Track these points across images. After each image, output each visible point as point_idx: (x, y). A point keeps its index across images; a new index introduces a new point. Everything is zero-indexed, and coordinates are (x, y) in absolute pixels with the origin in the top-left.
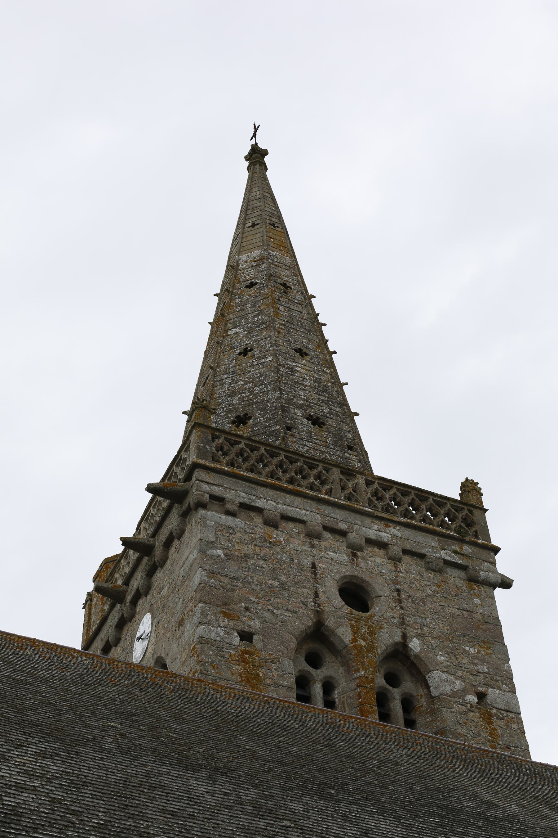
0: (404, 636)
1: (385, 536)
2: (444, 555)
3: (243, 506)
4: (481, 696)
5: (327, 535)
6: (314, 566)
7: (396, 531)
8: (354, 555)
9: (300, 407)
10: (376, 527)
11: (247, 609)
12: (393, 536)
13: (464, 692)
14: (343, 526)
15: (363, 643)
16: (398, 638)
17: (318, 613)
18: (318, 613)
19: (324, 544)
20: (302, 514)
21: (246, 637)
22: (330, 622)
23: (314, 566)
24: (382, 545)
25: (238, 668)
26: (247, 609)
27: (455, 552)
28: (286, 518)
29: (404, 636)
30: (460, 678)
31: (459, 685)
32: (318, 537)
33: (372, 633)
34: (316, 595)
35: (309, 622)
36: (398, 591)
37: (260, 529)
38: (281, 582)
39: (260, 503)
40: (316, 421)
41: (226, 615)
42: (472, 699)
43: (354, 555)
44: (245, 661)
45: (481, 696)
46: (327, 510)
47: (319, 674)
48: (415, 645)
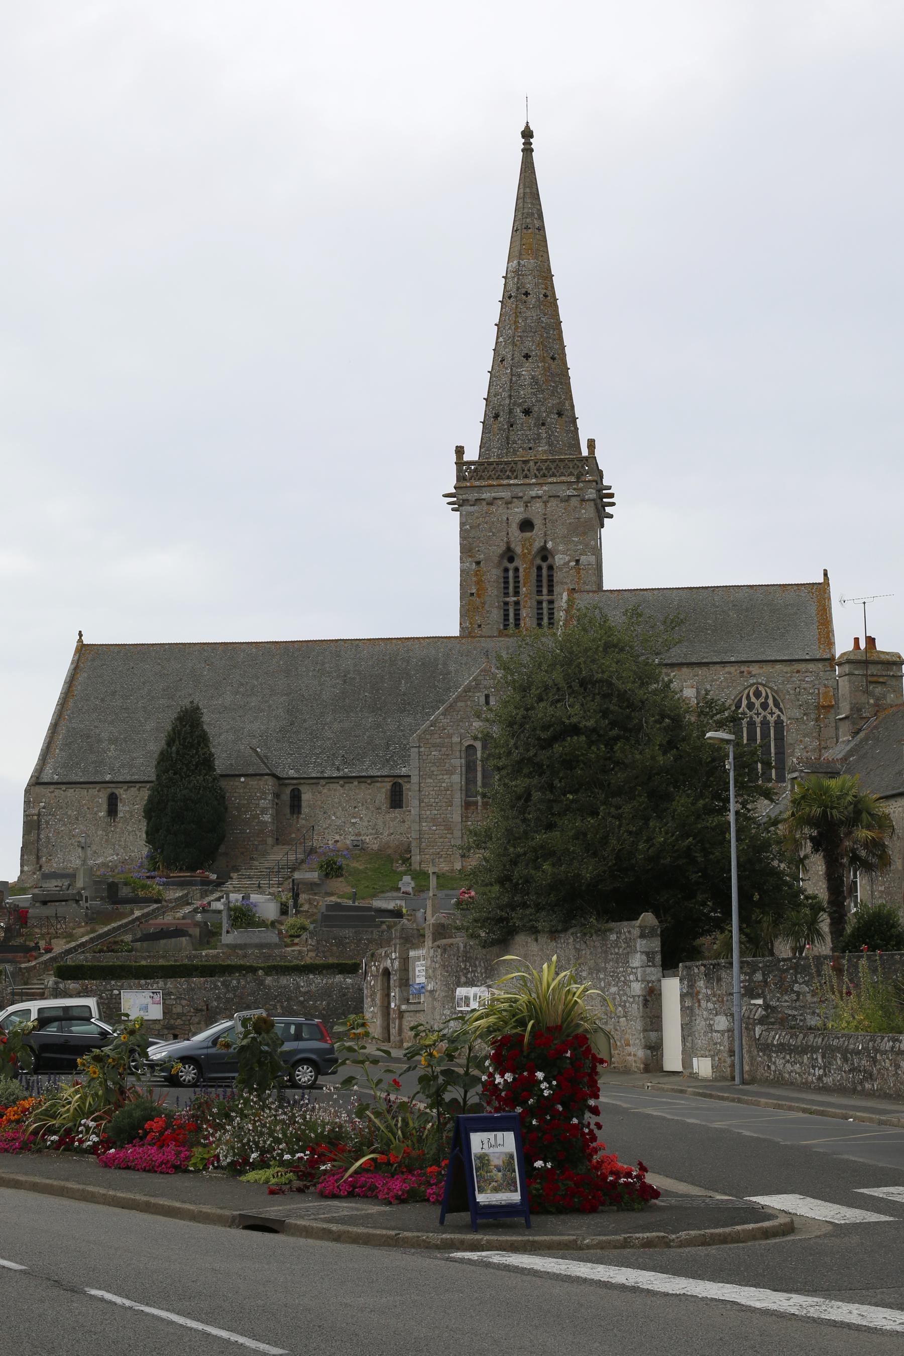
0: (545, 542)
1: (540, 493)
2: (568, 493)
3: (476, 500)
4: (577, 561)
5: (515, 500)
6: (508, 519)
7: (545, 488)
8: (527, 506)
9: (520, 405)
10: (536, 489)
11: (478, 551)
12: (545, 491)
13: (570, 561)
14: (520, 494)
15: (526, 551)
16: (542, 544)
17: (508, 543)
18: (508, 543)
19: (513, 505)
20: (502, 494)
21: (478, 563)
22: (512, 546)
23: (508, 519)
24: (539, 497)
25: (474, 579)
26: (478, 551)
27: (574, 489)
28: (495, 499)
29: (545, 542)
30: (569, 555)
31: (567, 558)
32: (511, 503)
33: (531, 545)
34: (508, 534)
35: (503, 547)
36: (545, 519)
37: (485, 508)
38: (493, 533)
39: (484, 496)
40: (527, 412)
41: (470, 556)
42: (573, 564)
43: (527, 506)
44: (476, 575)
45: (577, 561)
46: (513, 488)
47: (511, 566)
48: (550, 545)
